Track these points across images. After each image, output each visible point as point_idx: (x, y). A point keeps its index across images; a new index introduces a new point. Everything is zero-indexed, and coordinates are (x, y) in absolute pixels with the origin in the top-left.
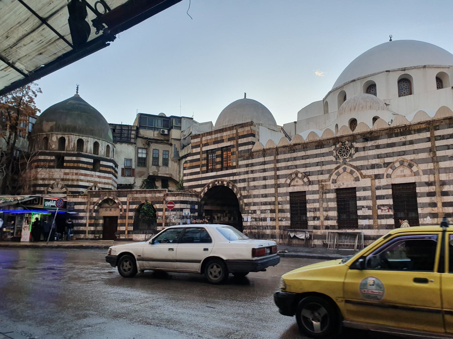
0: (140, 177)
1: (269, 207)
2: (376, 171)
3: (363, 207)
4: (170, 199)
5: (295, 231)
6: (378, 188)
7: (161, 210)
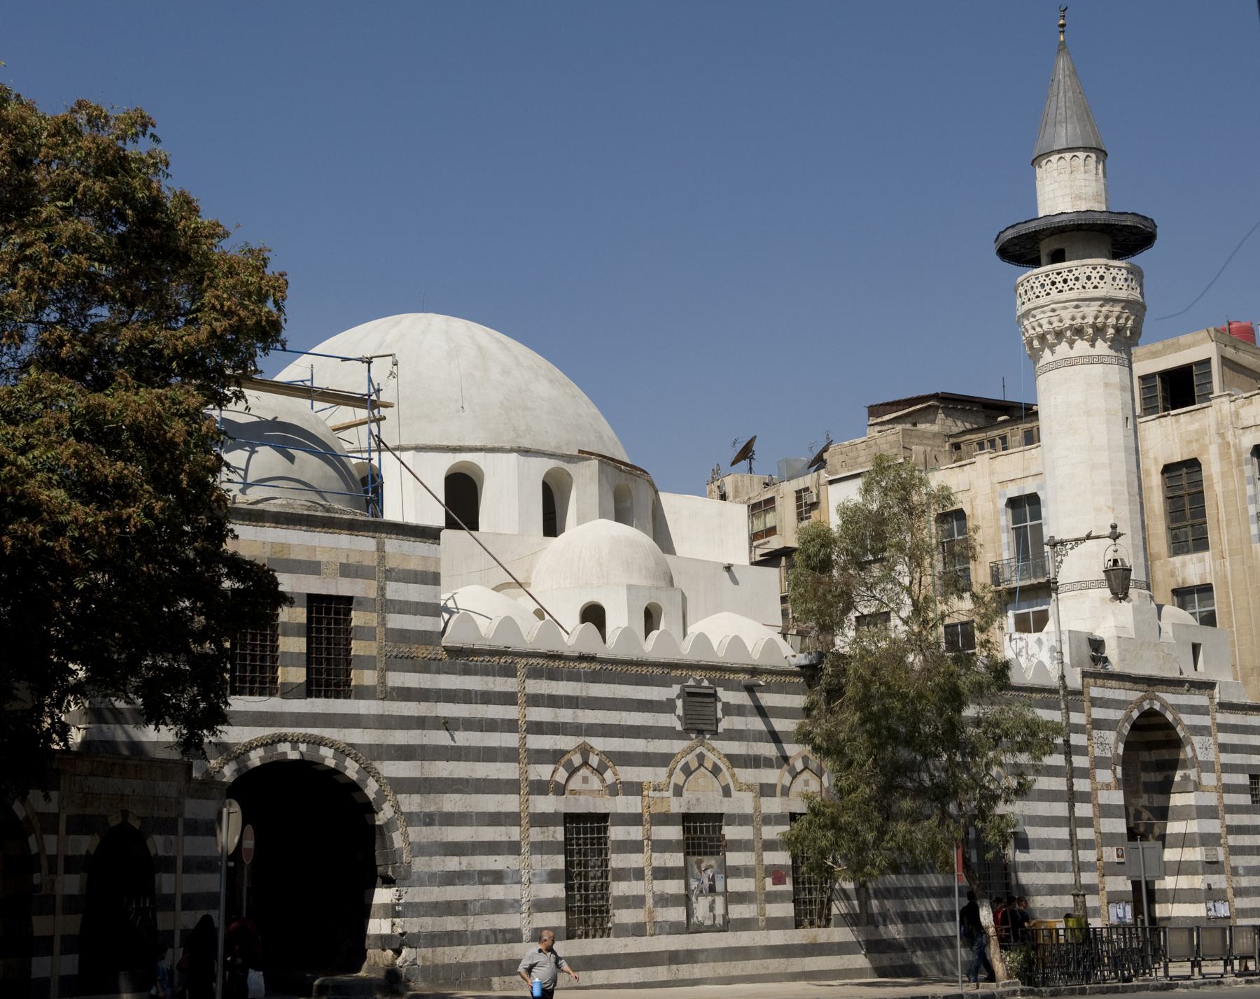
6: (768, 820)
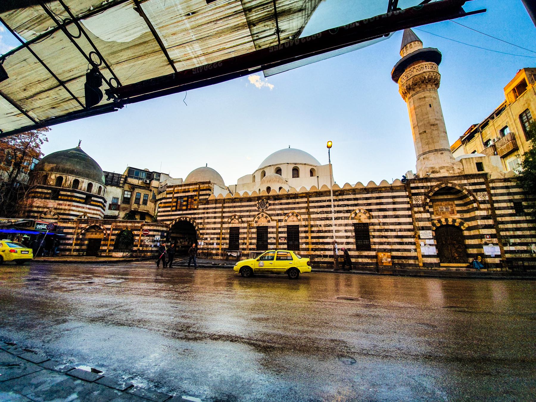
0: (124, 211)
1: (216, 236)
2: (279, 218)
3: (271, 238)
4: (146, 228)
5: (231, 252)
6: (280, 227)
7: (138, 235)
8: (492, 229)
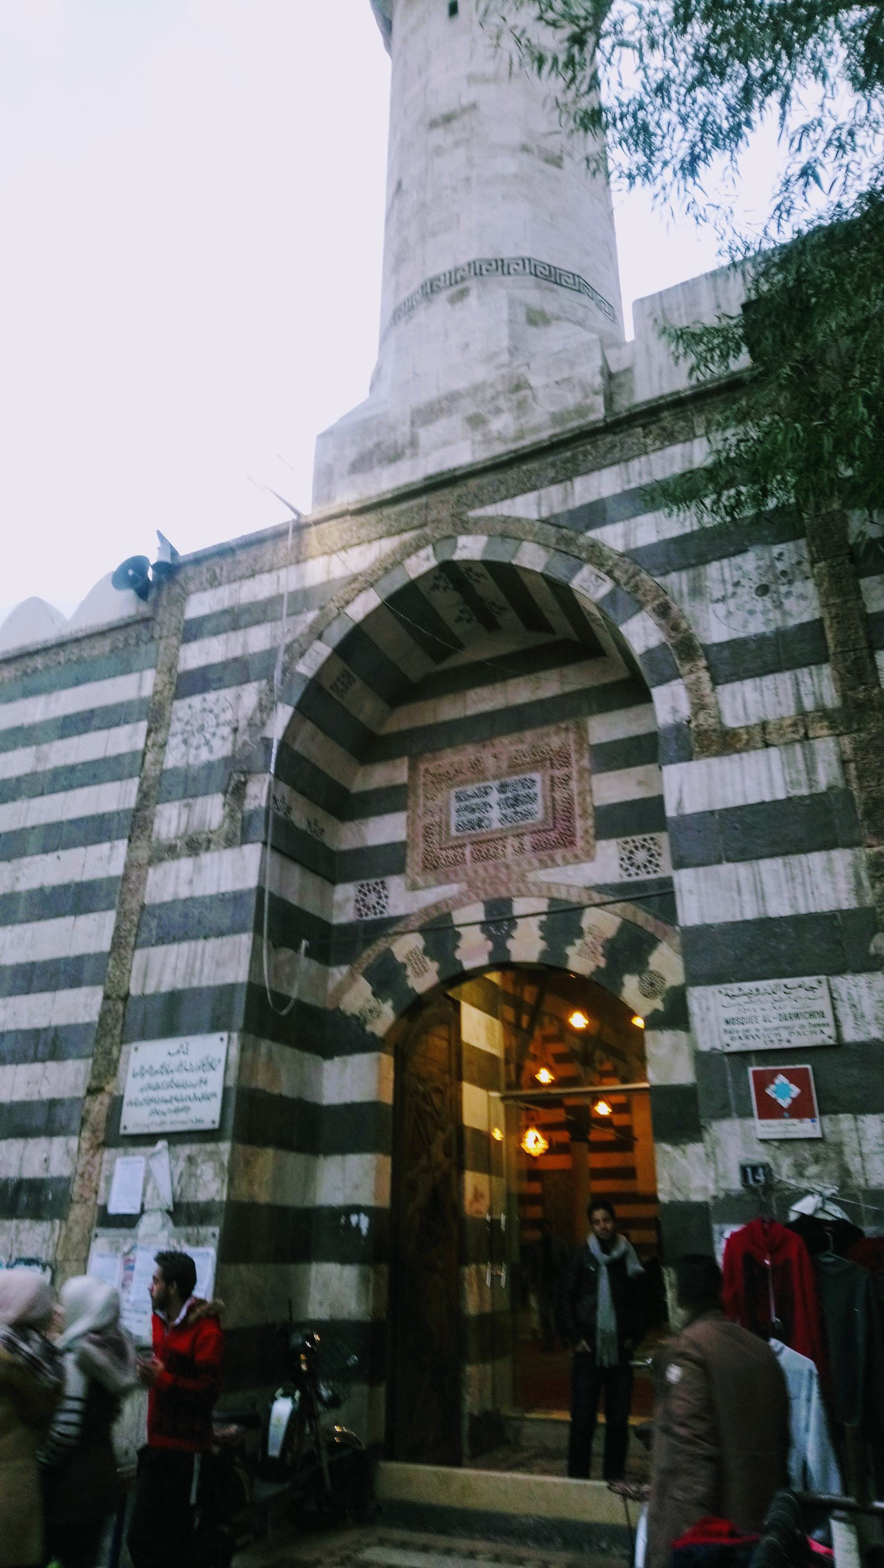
8: (845, 984)
